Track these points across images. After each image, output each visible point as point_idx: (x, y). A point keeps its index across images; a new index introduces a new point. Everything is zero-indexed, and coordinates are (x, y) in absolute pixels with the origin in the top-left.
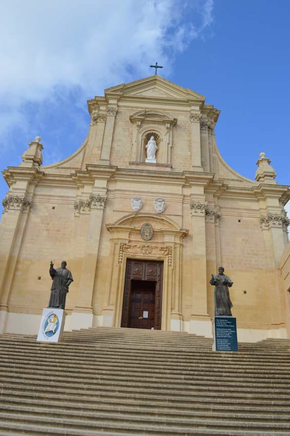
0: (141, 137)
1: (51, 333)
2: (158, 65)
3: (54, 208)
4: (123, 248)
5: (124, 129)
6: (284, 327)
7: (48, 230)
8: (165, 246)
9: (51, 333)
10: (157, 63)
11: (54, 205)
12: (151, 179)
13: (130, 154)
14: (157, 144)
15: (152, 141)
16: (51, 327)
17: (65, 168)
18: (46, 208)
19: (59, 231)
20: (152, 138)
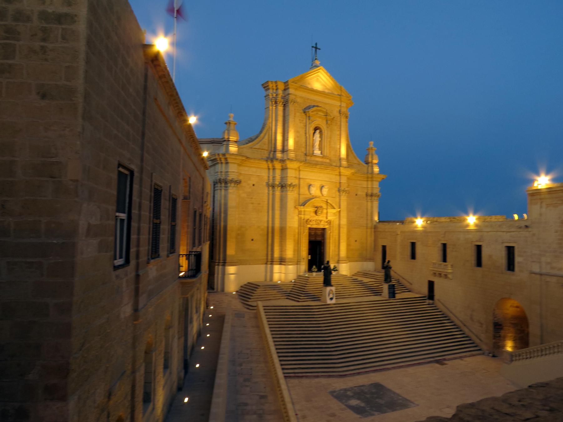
0: (312, 131)
1: (331, 299)
2: (318, 47)
3: (254, 185)
4: (307, 221)
5: (300, 120)
6: (373, 261)
7: (252, 203)
8: (327, 220)
9: (331, 299)
10: (316, 44)
11: (254, 183)
12: (320, 170)
13: (306, 145)
14: (321, 137)
15: (317, 135)
16: (331, 296)
17: (256, 149)
18: (249, 184)
19: (259, 204)
20: (318, 131)
